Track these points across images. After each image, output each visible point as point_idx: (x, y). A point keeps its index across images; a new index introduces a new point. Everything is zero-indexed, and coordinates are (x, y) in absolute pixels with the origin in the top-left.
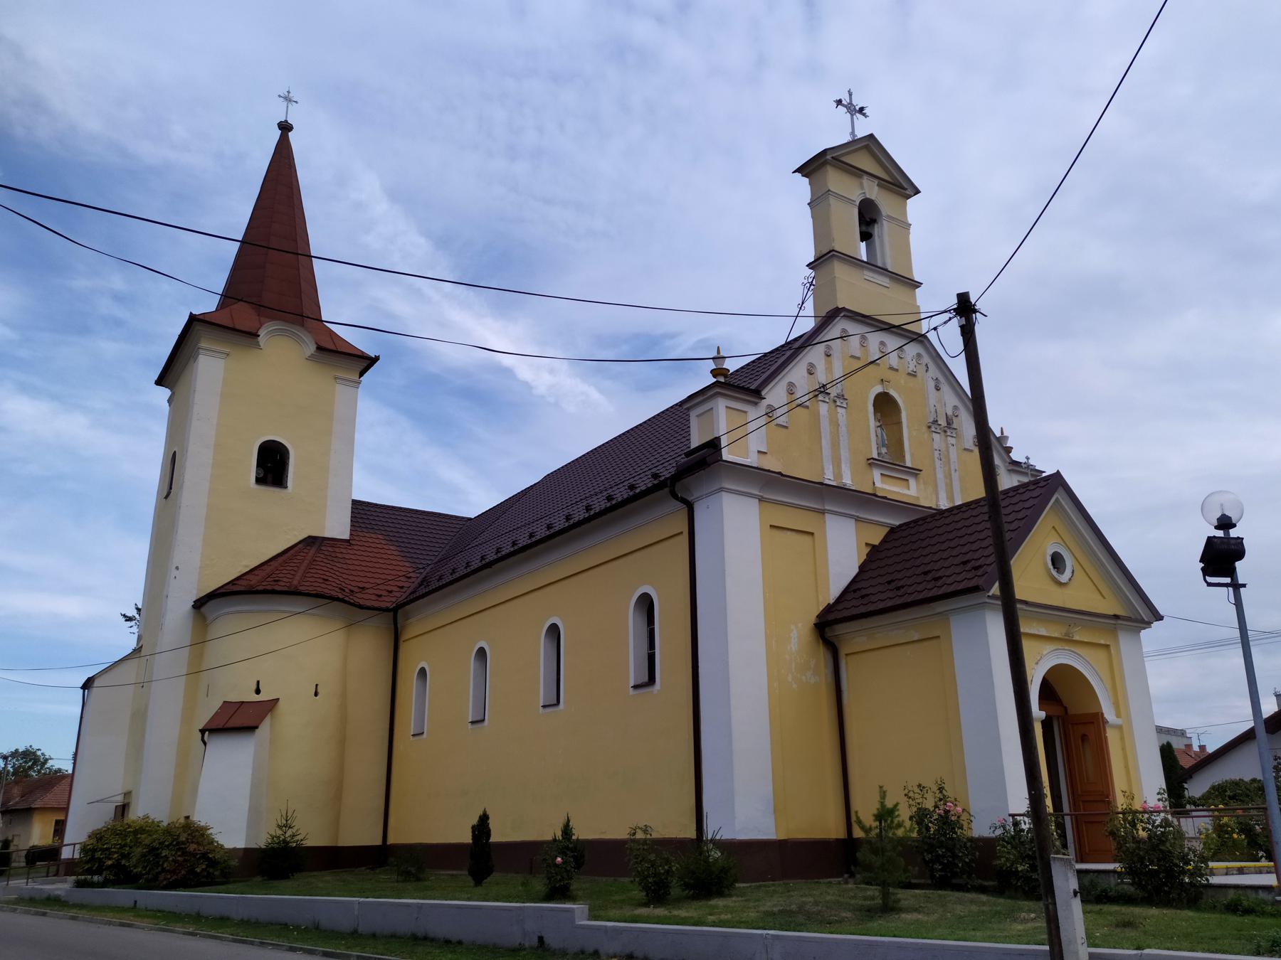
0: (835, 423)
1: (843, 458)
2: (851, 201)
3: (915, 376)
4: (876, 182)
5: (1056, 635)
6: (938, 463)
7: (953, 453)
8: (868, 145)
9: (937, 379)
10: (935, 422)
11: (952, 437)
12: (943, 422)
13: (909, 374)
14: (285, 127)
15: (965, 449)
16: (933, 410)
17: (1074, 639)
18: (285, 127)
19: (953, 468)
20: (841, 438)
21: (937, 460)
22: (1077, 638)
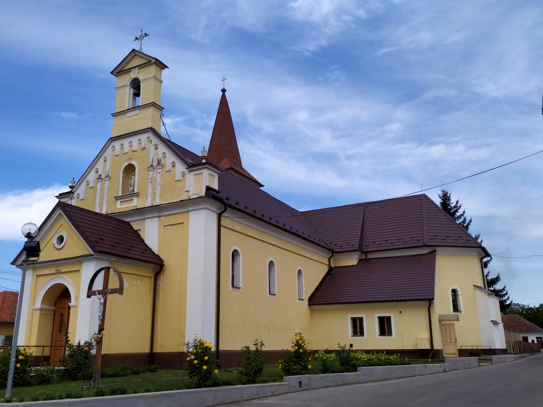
0: (103, 188)
1: (104, 202)
2: (125, 86)
3: (145, 149)
4: (137, 68)
5: (54, 272)
6: (150, 184)
7: (159, 177)
8: (135, 54)
9: (156, 144)
10: (152, 166)
11: (159, 169)
12: (155, 164)
13: (142, 149)
14: (224, 91)
15: (166, 172)
16: (151, 160)
17: (62, 271)
18: (224, 91)
19: (157, 184)
20: (105, 194)
21: (149, 183)
22: (63, 271)
